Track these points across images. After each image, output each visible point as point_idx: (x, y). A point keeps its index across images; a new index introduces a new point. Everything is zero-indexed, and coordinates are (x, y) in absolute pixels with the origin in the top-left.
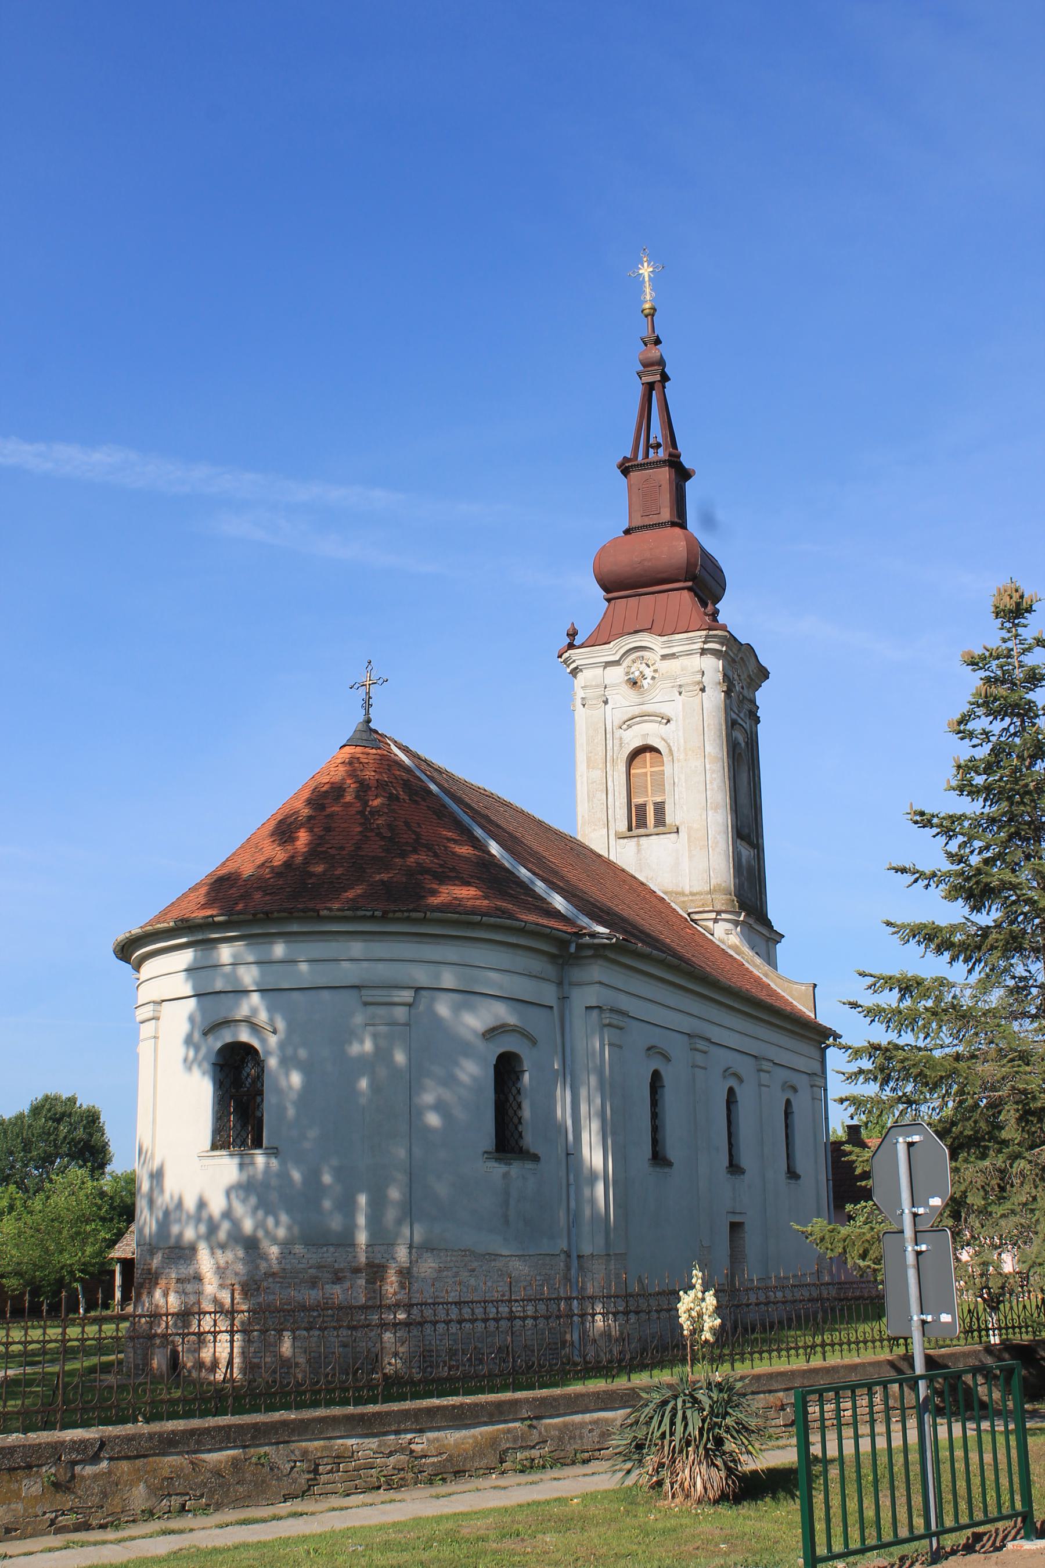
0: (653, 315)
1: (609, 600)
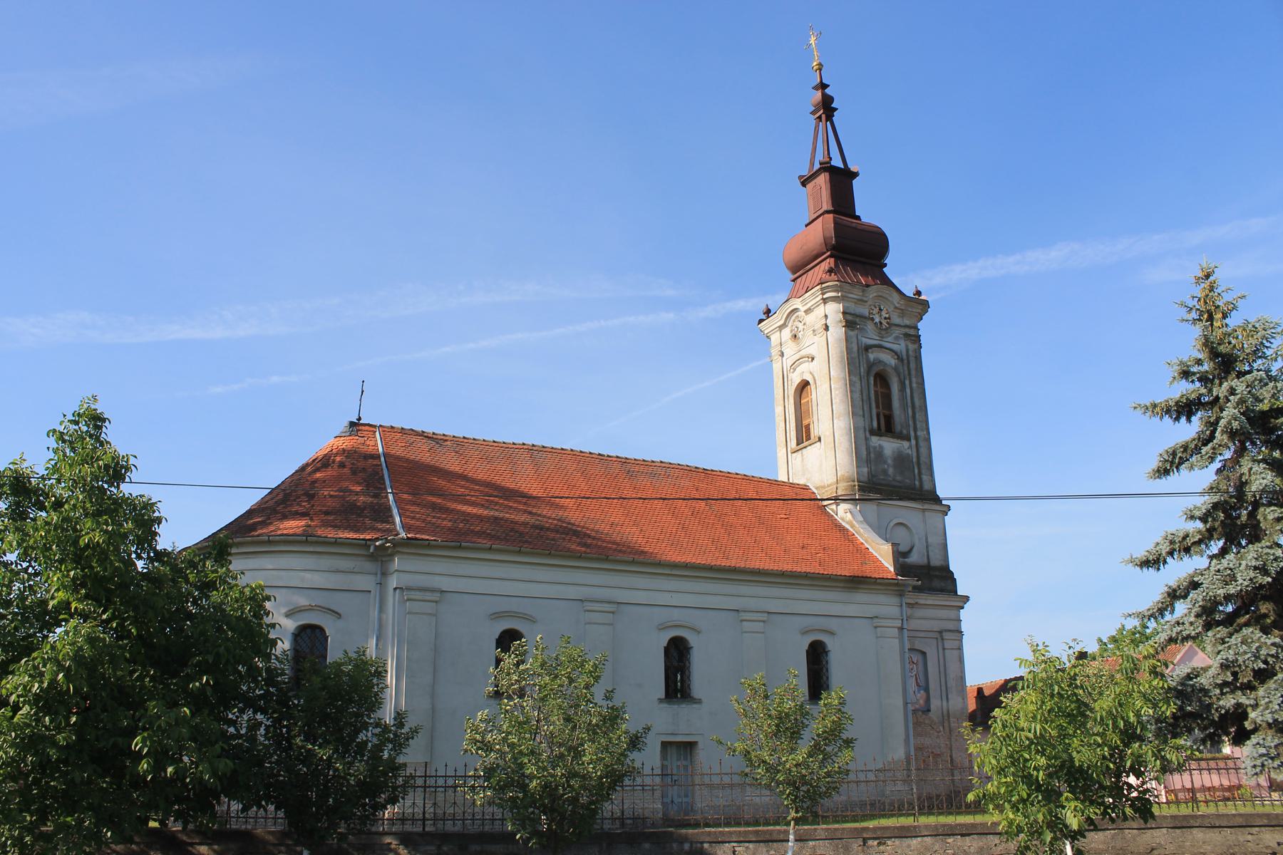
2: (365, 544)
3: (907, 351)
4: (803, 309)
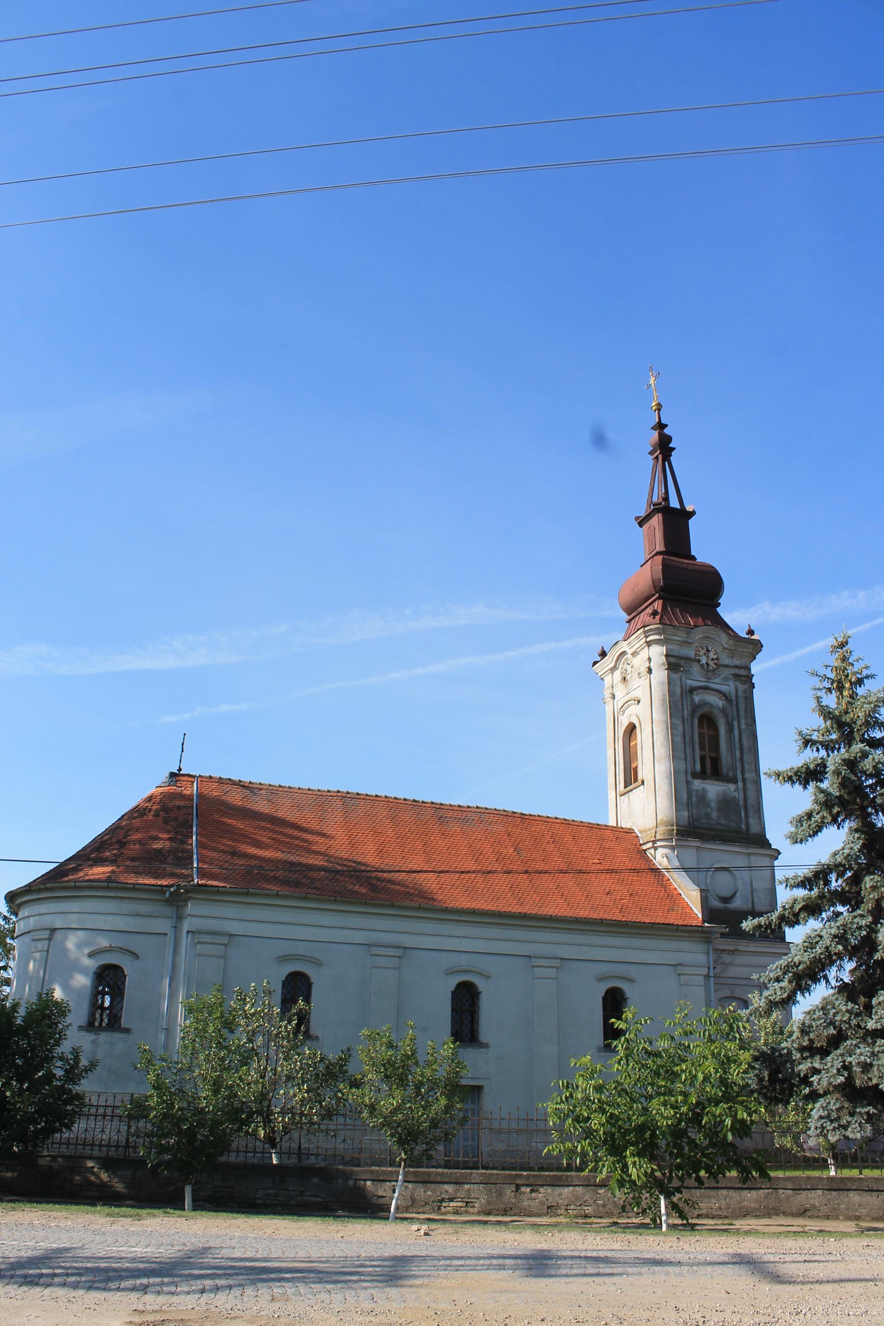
0: (659, 410)
2: (162, 889)
3: (737, 691)
4: (630, 652)
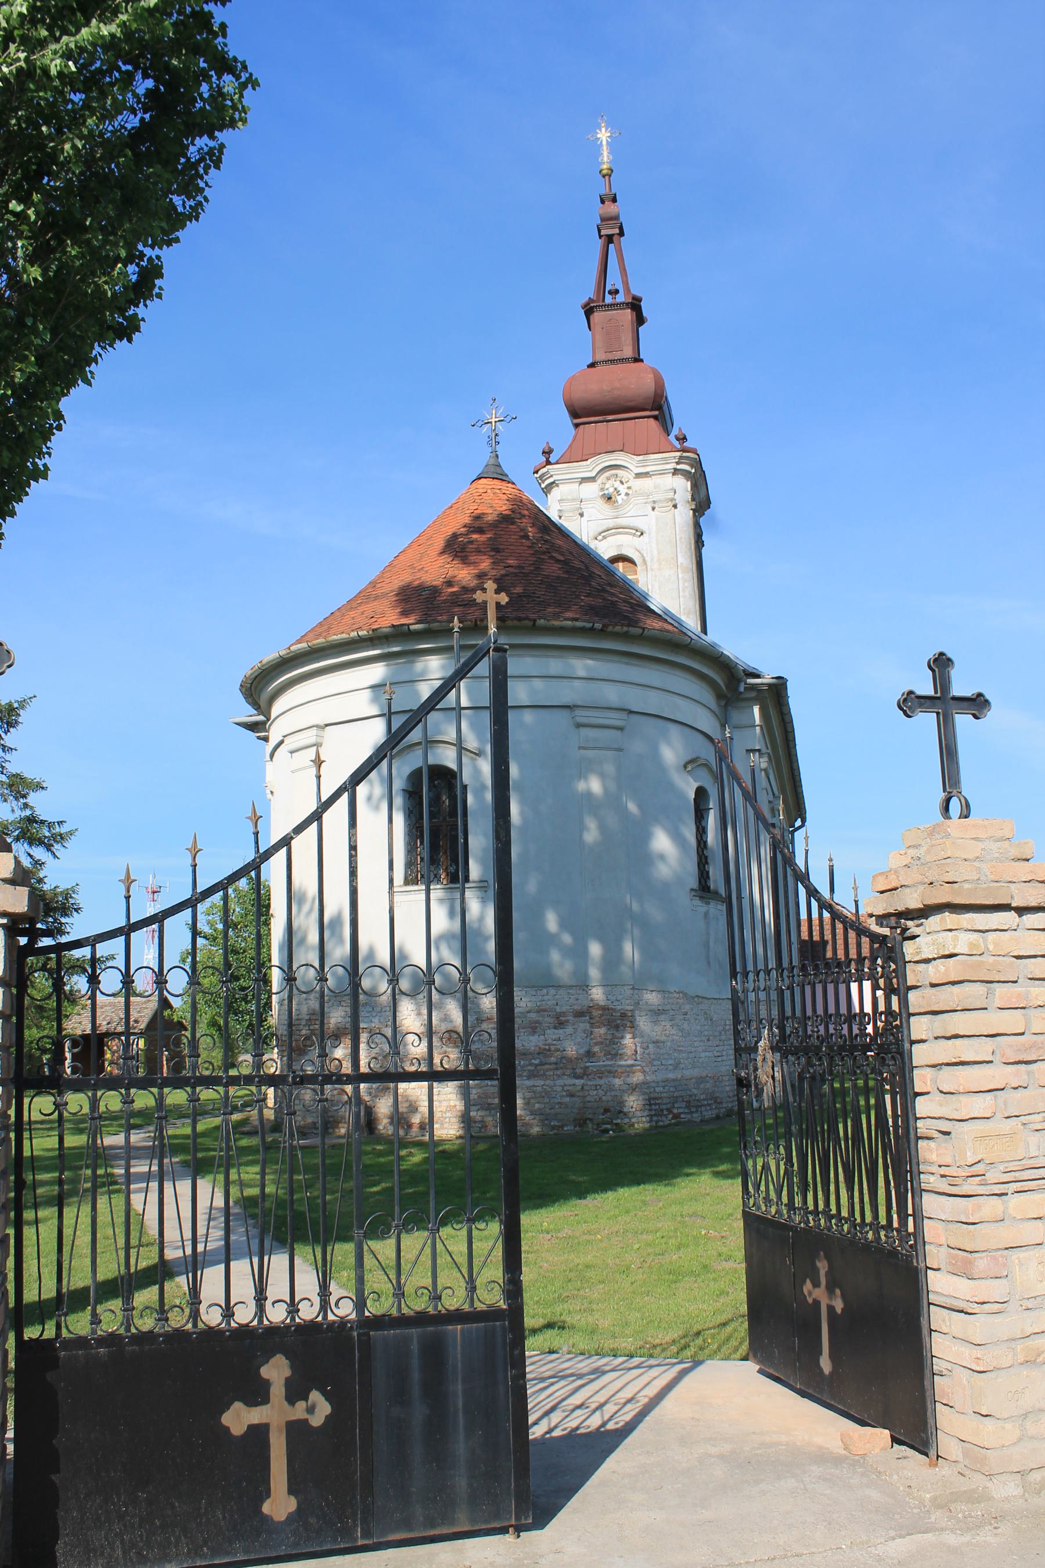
1: (577, 426)
